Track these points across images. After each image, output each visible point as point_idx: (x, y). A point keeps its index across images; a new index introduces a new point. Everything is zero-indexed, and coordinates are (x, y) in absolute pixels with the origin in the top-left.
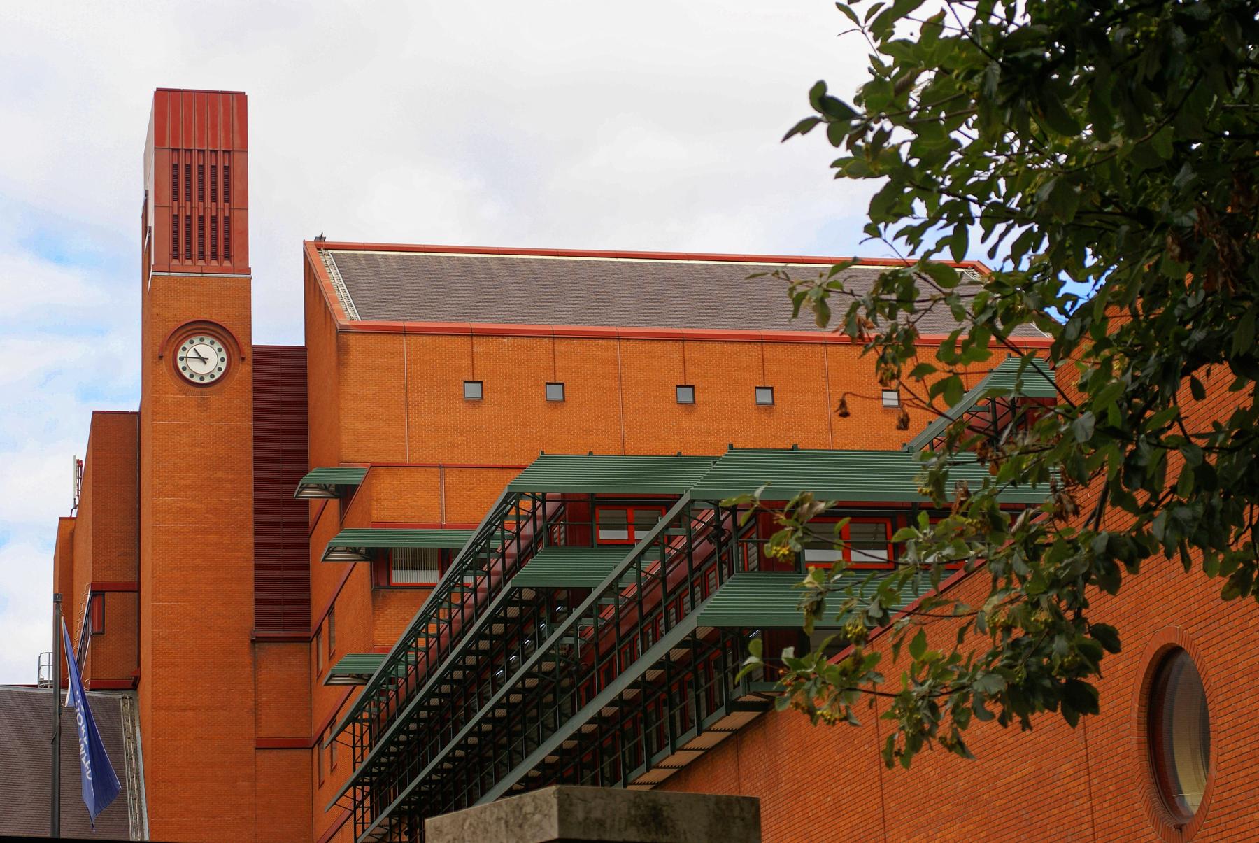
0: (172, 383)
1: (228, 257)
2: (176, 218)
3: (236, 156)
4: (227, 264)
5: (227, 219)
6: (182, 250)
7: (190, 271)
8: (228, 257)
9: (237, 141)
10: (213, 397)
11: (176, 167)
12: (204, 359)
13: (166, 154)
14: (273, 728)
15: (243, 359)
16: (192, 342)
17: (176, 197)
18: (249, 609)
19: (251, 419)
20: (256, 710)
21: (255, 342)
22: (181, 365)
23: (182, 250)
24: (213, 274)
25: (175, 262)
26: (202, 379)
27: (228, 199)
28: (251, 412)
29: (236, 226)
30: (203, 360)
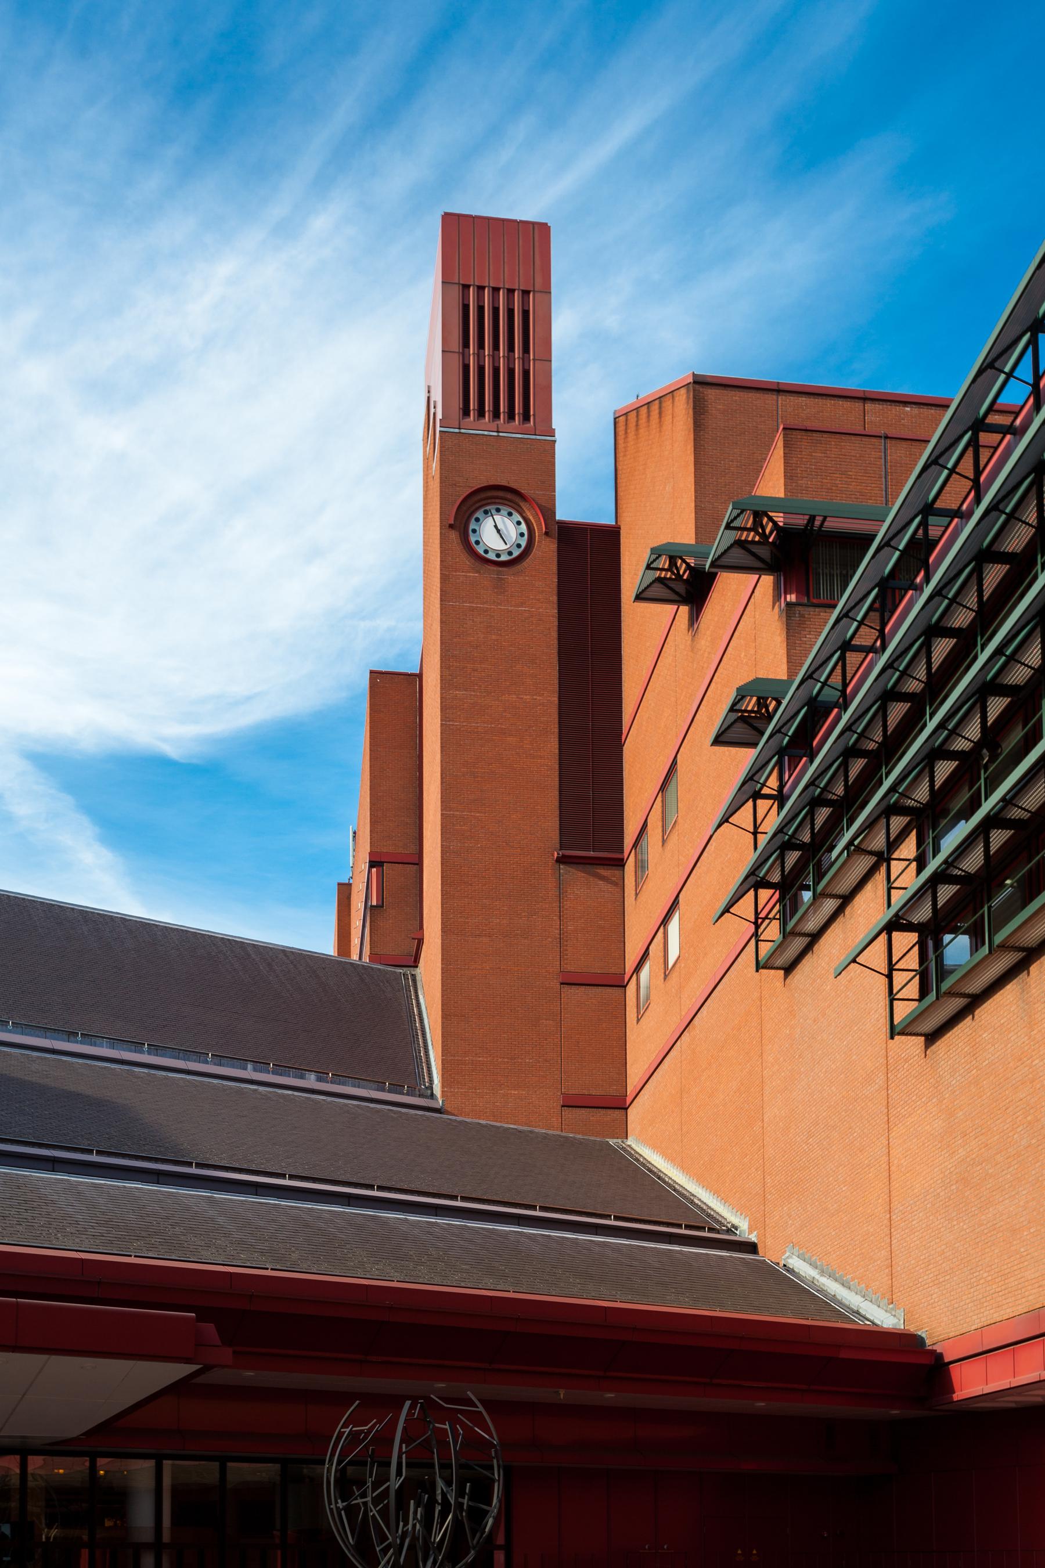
0: (465, 560)
1: (526, 417)
6: (473, 404)
7: (483, 428)
10: (511, 578)
12: (498, 533)
13: (455, 292)
14: (581, 962)
18: (552, 824)
19: (556, 606)
20: (561, 940)
21: (559, 517)
23: (473, 404)
24: (512, 432)
26: (498, 556)
28: (554, 598)
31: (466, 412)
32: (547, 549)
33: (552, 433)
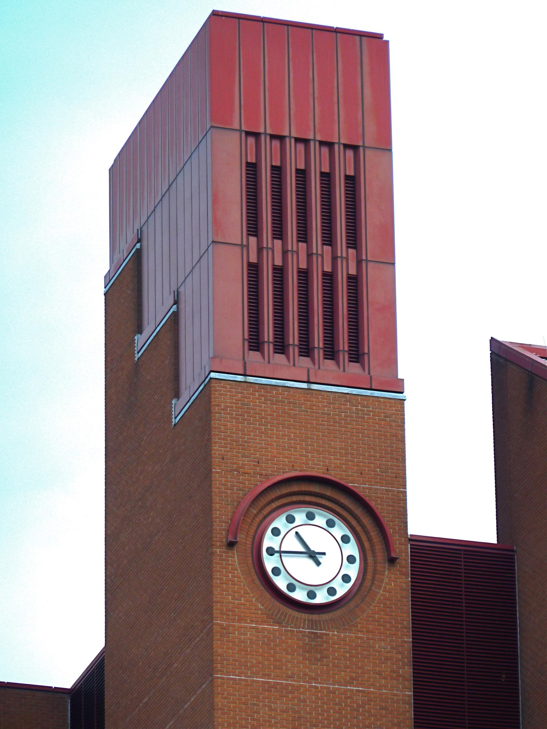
1: (357, 355)
2: (254, 271)
3: (370, 157)
4: (354, 369)
5: (355, 282)
6: (268, 333)
8: (357, 355)
9: (371, 128)
11: (252, 169)
15: (392, 561)
16: (291, 519)
17: (253, 227)
19: (410, 684)
22: (270, 563)
23: (268, 333)
25: (254, 356)
27: (354, 240)
28: (408, 671)
29: (371, 295)
30: (314, 556)
31: (255, 343)
32: (397, 584)
33: (398, 386)
